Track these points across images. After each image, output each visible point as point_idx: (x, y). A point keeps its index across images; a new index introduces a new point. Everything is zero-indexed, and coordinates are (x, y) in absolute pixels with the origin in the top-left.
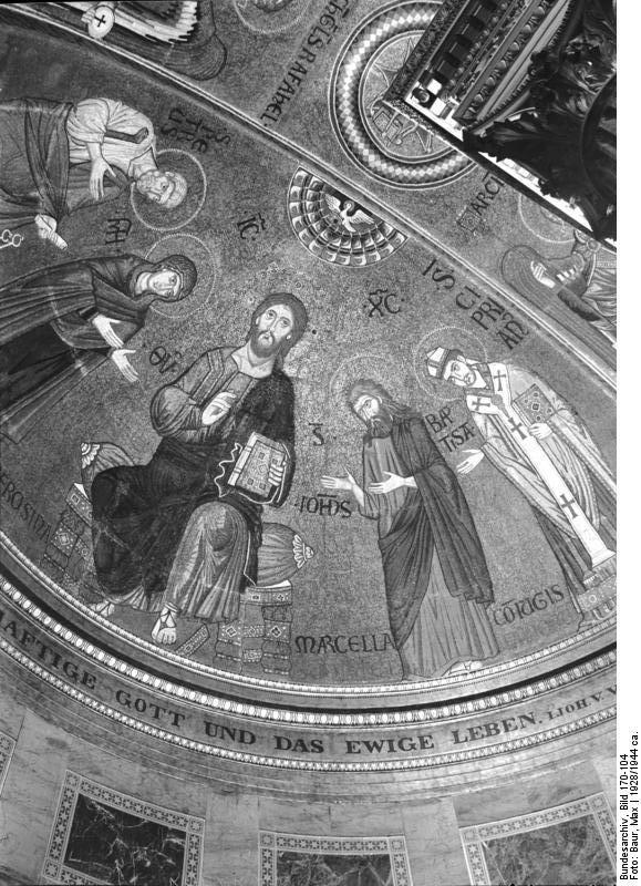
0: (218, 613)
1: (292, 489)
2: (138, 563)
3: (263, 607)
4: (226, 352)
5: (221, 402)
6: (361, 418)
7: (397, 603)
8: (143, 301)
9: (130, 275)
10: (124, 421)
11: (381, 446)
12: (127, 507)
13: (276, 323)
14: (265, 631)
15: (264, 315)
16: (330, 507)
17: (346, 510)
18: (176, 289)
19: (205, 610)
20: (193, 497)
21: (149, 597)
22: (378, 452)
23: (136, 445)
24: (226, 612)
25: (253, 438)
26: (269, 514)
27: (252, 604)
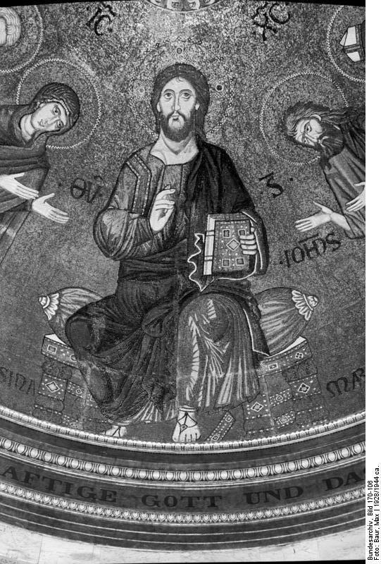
0: (239, 396)
1: (271, 249)
2: (140, 383)
3: (283, 372)
4: (144, 153)
5: (164, 203)
6: (308, 146)
8: (37, 146)
9: (11, 126)
10: (74, 262)
12: (110, 338)
14: (291, 393)
15: (162, 99)
16: (315, 248)
17: (333, 242)
18: (63, 118)
19: (224, 398)
20: (175, 302)
21: (161, 408)
22: (341, 169)
24: (247, 392)
25: (211, 222)
26: (258, 284)
27: (271, 374)
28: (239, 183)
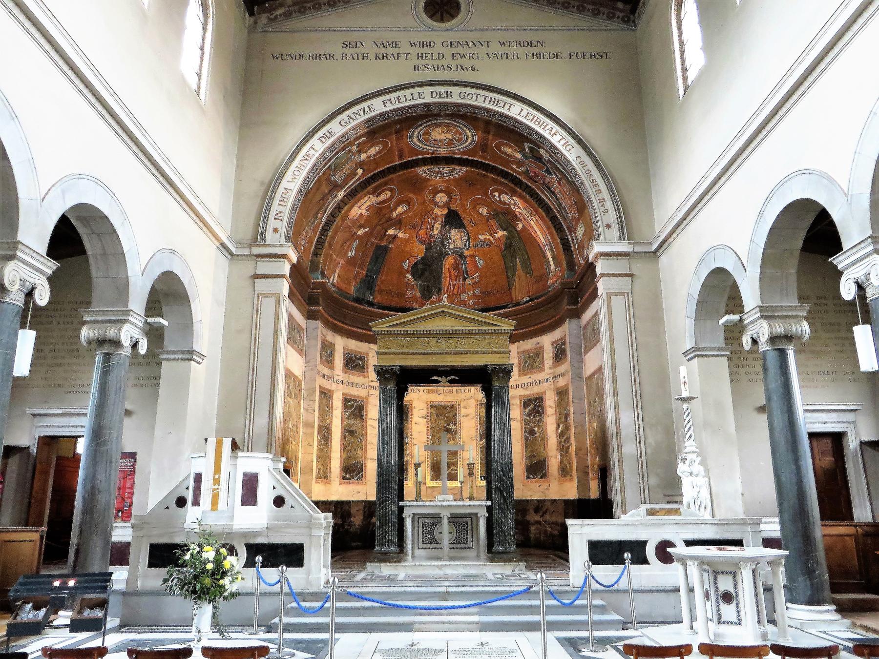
4: (431, 212)
5: (438, 226)
7: (509, 275)
8: (398, 219)
9: (390, 217)
11: (492, 222)
12: (424, 270)
13: (441, 198)
18: (405, 209)
19: (455, 292)
23: (419, 251)
25: (453, 231)
26: (467, 253)
27: (468, 284)
28: (461, 221)
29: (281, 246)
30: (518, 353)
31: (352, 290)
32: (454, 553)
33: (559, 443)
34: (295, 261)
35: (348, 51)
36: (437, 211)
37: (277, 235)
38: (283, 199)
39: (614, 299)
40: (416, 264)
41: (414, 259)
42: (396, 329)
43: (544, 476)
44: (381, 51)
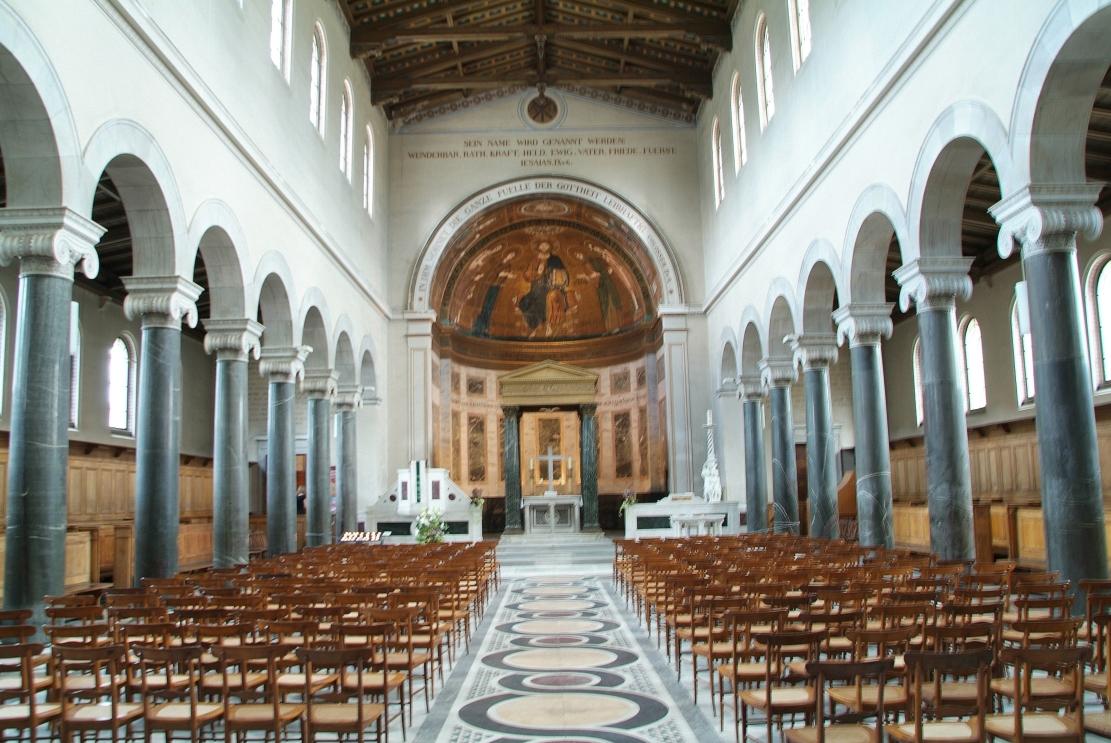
11: (588, 266)
12: (530, 304)
23: (526, 288)
25: (554, 271)
26: (567, 289)
29: (426, 312)
30: (611, 376)
31: (471, 325)
32: (558, 530)
33: (640, 451)
34: (435, 320)
35: (469, 150)
36: (541, 256)
37: (422, 303)
38: (425, 275)
39: (674, 349)
40: (523, 299)
41: (521, 295)
42: (517, 379)
43: (629, 475)
44: (495, 149)
